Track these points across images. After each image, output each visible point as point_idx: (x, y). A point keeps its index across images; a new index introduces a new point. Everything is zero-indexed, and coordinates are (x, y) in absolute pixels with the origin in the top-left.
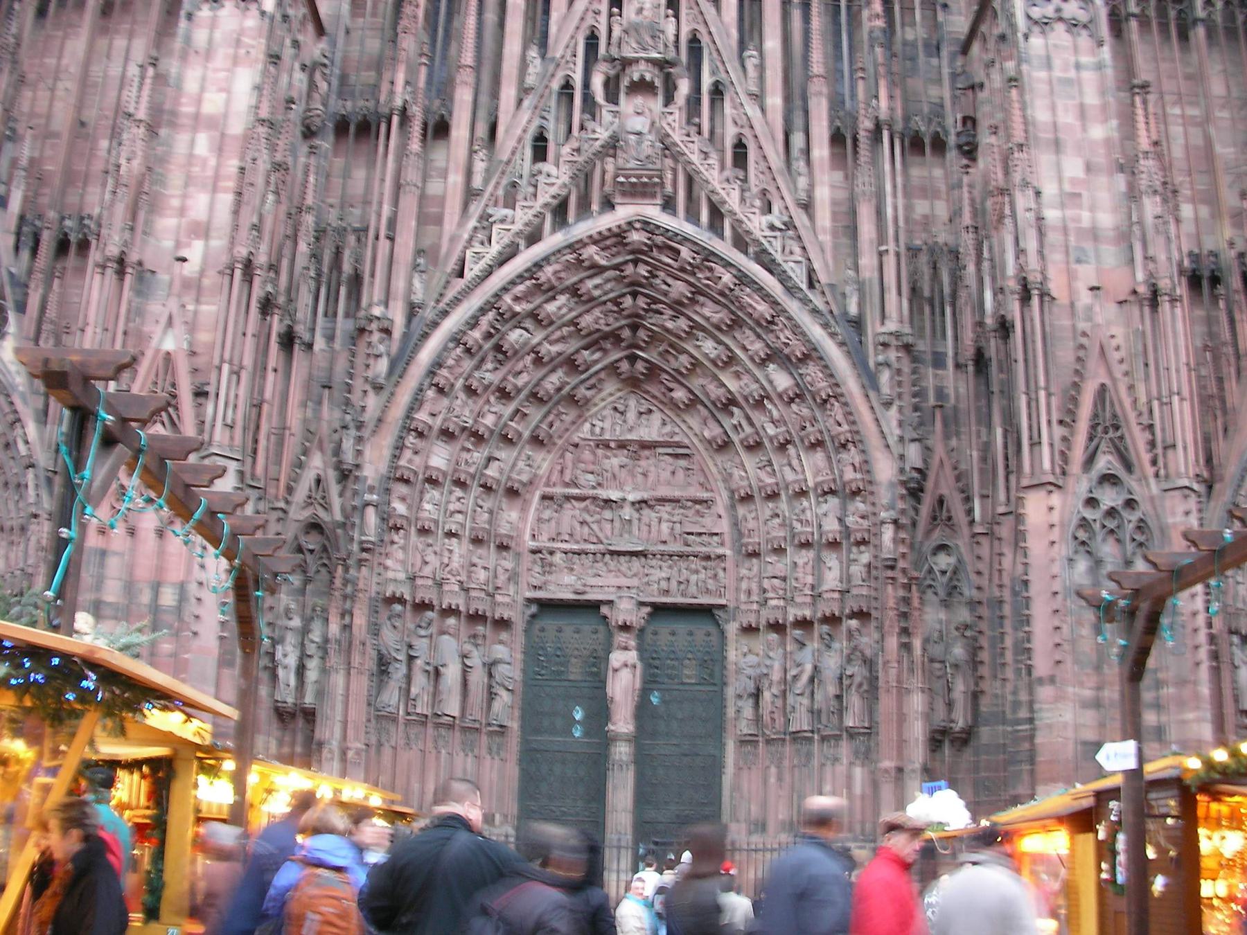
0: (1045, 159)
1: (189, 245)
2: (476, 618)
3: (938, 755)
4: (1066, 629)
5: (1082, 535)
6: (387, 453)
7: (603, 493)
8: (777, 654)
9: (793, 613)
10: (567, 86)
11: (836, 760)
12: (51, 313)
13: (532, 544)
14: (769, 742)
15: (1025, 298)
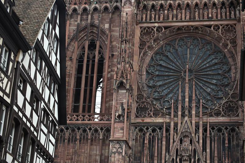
10: (173, 159)
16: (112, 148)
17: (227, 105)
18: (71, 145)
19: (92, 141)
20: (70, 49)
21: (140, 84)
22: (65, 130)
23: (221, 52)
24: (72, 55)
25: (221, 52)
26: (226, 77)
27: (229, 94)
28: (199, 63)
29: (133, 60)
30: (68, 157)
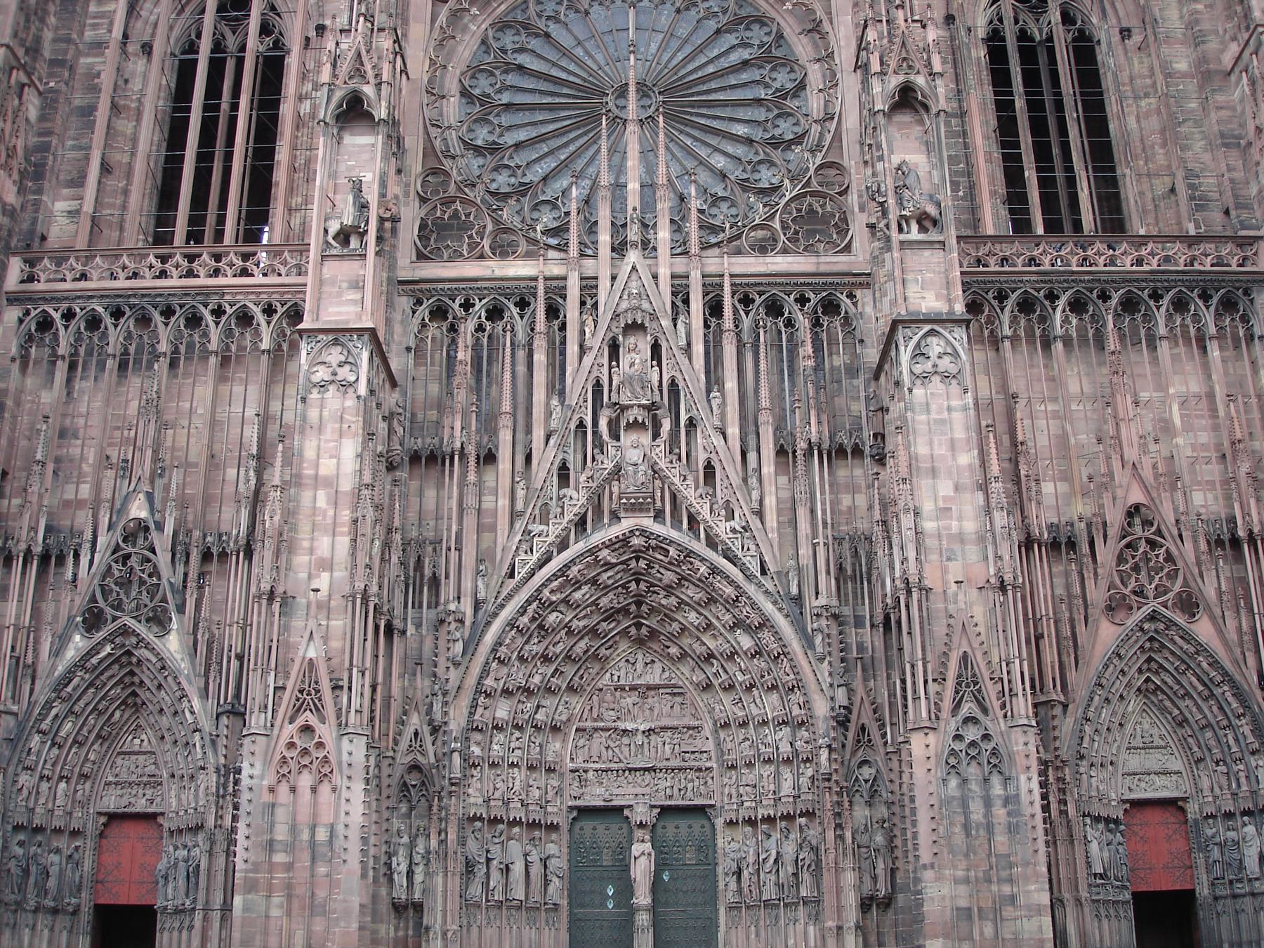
0: (924, 484)
1: (319, 576)
2: (533, 825)
3: (868, 916)
4: (941, 829)
5: (952, 761)
6: (465, 711)
7: (622, 725)
8: (751, 842)
9: (761, 812)
10: (581, 425)
11: (796, 921)
12: (204, 613)
13: (571, 766)
14: (748, 907)
15: (909, 592)
16: (312, 365)
17: (799, 210)
18: (135, 382)
19: (225, 361)
20: (142, 13)
21: (434, 132)
22: (108, 321)
23: (761, 21)
24: (153, 35)
25: (763, 24)
26: (784, 115)
27: (808, 168)
28: (674, 62)
29: (404, 35)
30: (118, 434)
